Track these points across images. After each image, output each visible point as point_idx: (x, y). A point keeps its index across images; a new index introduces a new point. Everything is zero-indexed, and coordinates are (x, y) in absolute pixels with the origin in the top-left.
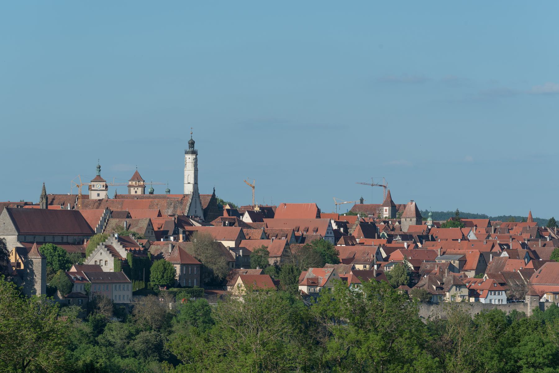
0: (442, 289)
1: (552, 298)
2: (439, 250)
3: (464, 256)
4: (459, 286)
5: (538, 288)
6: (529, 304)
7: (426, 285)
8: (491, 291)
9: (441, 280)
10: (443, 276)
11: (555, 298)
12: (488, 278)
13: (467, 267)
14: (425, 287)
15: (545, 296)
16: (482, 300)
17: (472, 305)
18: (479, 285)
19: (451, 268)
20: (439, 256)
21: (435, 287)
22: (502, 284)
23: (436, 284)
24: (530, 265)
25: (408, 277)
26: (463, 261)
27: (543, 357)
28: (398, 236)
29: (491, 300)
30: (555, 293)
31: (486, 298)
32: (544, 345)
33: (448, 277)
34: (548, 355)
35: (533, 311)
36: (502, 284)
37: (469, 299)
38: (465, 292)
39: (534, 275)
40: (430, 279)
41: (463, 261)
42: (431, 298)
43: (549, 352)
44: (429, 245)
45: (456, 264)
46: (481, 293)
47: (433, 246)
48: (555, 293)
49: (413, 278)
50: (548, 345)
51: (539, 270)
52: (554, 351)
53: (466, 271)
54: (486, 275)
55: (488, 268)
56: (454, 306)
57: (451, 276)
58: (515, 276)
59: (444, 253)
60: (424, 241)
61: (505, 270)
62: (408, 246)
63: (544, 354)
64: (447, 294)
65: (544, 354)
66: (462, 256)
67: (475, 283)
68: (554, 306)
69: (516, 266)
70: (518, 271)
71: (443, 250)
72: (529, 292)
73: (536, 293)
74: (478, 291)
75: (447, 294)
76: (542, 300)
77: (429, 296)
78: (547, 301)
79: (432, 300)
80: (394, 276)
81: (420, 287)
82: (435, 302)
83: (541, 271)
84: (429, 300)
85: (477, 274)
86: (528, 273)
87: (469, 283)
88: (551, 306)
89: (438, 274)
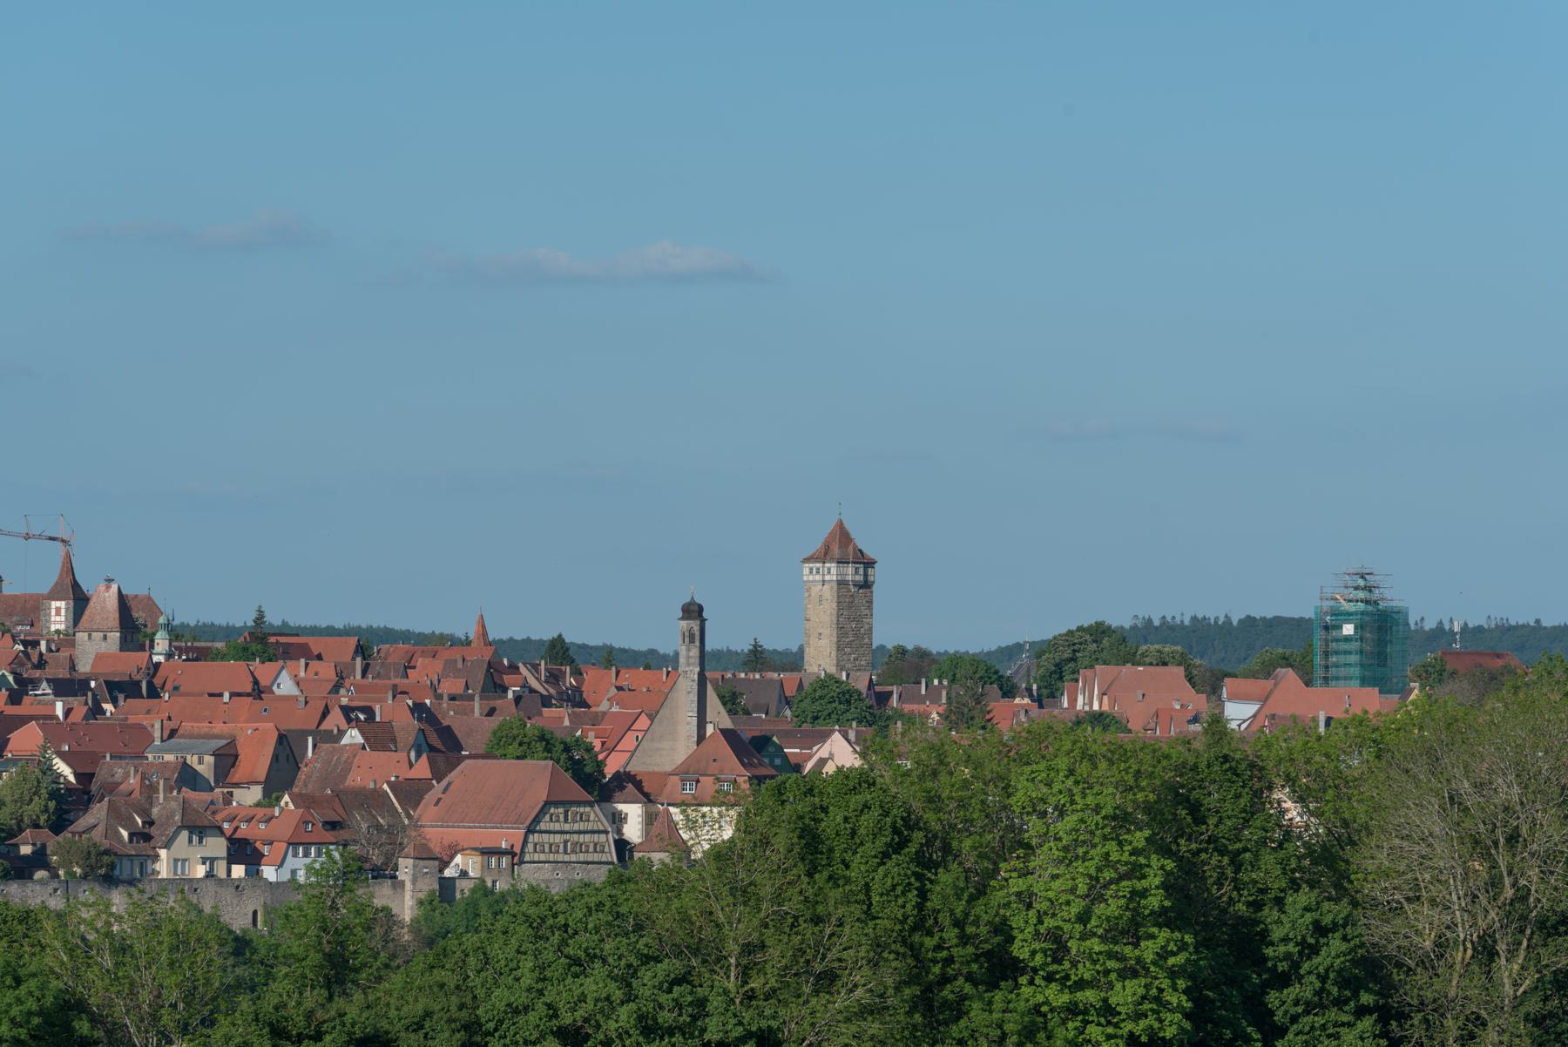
0: (147, 838)
1: (478, 866)
2: (158, 726)
3: (232, 743)
4: (199, 830)
5: (436, 836)
6: (408, 885)
7: (101, 829)
8: (296, 845)
9: (145, 813)
10: (150, 800)
11: (486, 867)
12: (291, 806)
13: (238, 774)
14: (97, 835)
15: (458, 859)
16: (269, 873)
17: (237, 886)
18: (262, 826)
19: (188, 777)
20: (158, 742)
21: (125, 834)
22: (333, 825)
23: (128, 823)
24: (422, 769)
25: (52, 804)
26: (227, 759)
27: (12, 1020)
28: (44, 685)
29: (294, 872)
30: (487, 852)
31: (281, 865)
32: (18, 981)
33: (166, 804)
34: (30, 1013)
35: (421, 903)
36: (333, 825)
37: (229, 872)
38: (217, 846)
39: (429, 798)
40: (112, 808)
41: (227, 759)
42: (112, 866)
43: (32, 1005)
44: (135, 710)
45: (205, 766)
46: (266, 850)
47: (148, 712)
48: (487, 852)
49: (65, 806)
50: (32, 984)
51: (444, 782)
52: (49, 1001)
53: (237, 785)
54: (286, 798)
55: (302, 776)
56: (184, 885)
57: (176, 799)
58: (372, 800)
59: (173, 734)
60: (121, 697)
61: (349, 782)
62: (67, 713)
63: (15, 1011)
64: (163, 853)
65: (15, 1011)
66: (224, 742)
67: (249, 820)
68: (482, 890)
69: (378, 772)
70: (385, 787)
71: (169, 725)
72: (409, 850)
73: (430, 850)
74: (258, 845)
75: (163, 853)
76: (448, 873)
77: (106, 859)
78: (464, 874)
79: (117, 872)
80: (8, 799)
81: (80, 835)
82: (125, 876)
83: (449, 784)
84: (107, 869)
85: (267, 793)
86: (411, 793)
87: (231, 821)
88: (473, 891)
89: (137, 794)
